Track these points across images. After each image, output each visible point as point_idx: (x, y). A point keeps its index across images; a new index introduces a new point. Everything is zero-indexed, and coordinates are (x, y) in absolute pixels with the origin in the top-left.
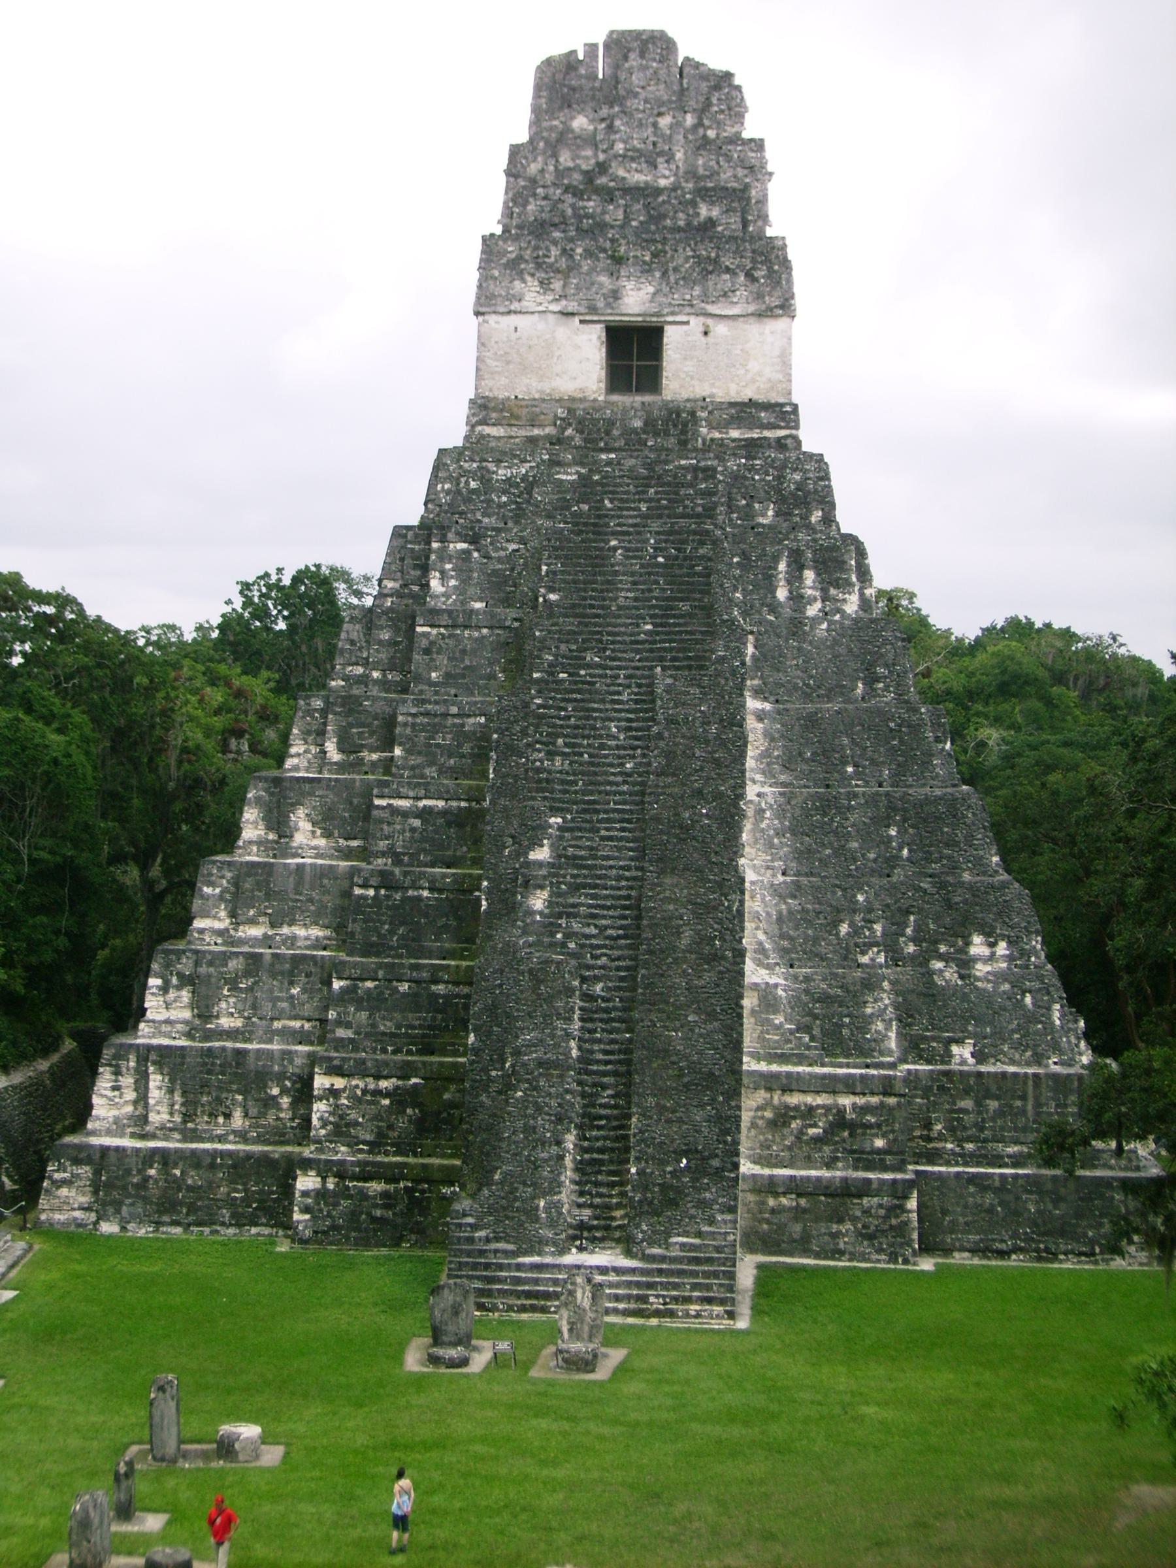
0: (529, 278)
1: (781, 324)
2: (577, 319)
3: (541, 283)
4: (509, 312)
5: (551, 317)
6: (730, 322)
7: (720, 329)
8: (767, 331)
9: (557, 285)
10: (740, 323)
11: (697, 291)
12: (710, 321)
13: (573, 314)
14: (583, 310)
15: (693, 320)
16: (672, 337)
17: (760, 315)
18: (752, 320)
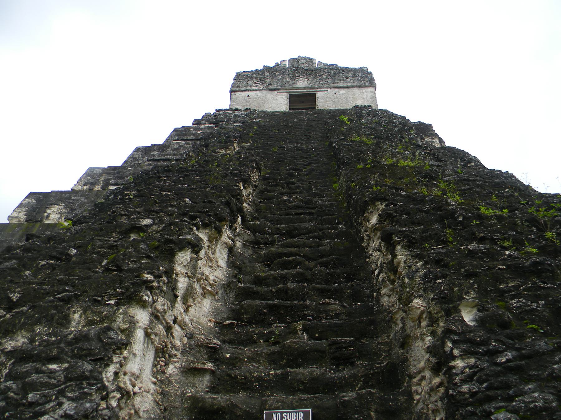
0: (254, 79)
1: (371, 89)
2: (276, 92)
3: (260, 80)
4: (245, 91)
5: (264, 92)
6: (347, 90)
7: (342, 92)
8: (364, 91)
9: (268, 81)
10: (351, 90)
11: (330, 81)
12: (336, 90)
13: (275, 90)
14: (279, 87)
15: (329, 90)
16: (320, 95)
17: (360, 87)
18: (355, 88)
